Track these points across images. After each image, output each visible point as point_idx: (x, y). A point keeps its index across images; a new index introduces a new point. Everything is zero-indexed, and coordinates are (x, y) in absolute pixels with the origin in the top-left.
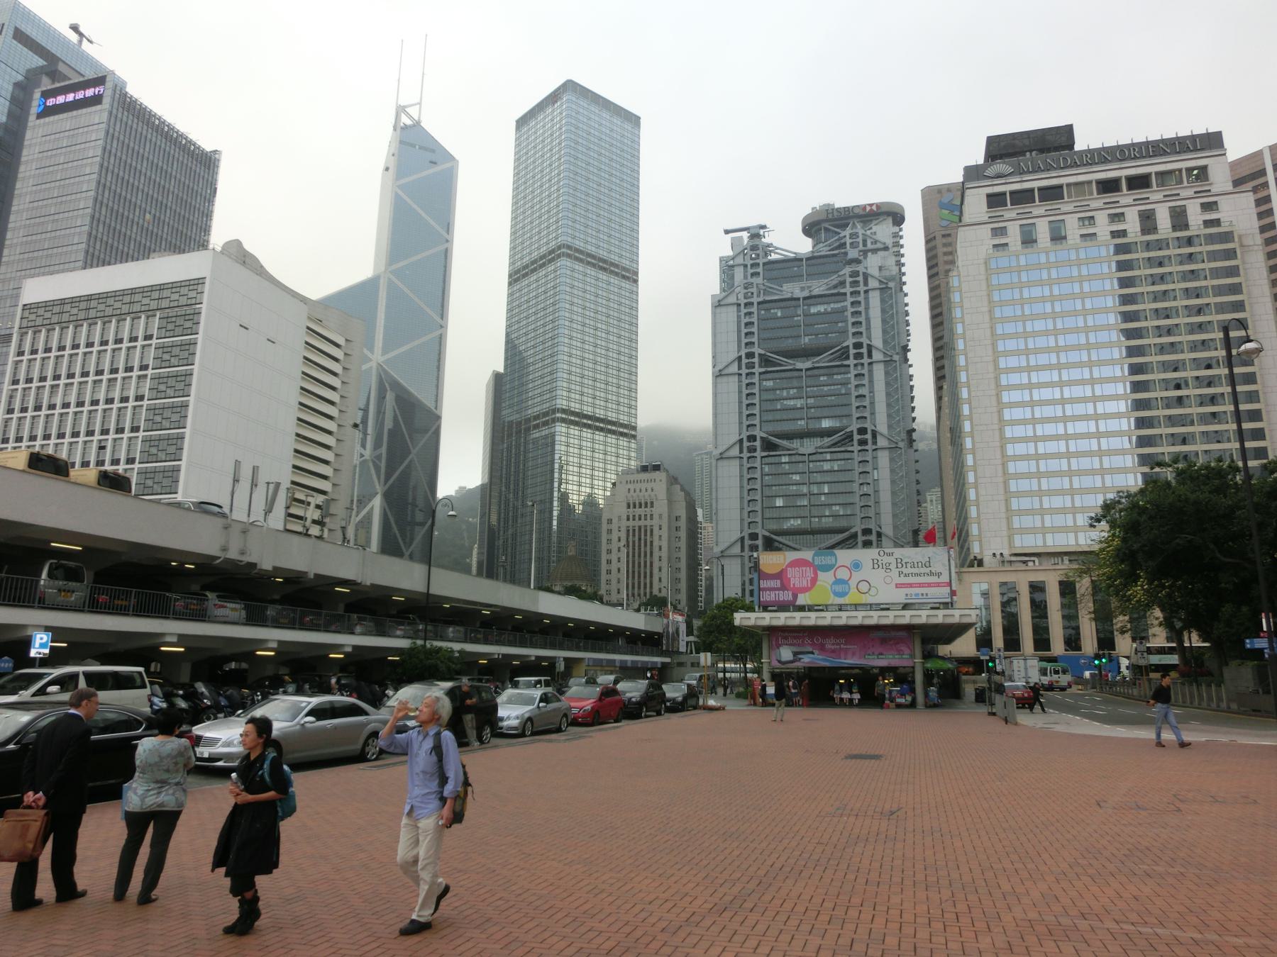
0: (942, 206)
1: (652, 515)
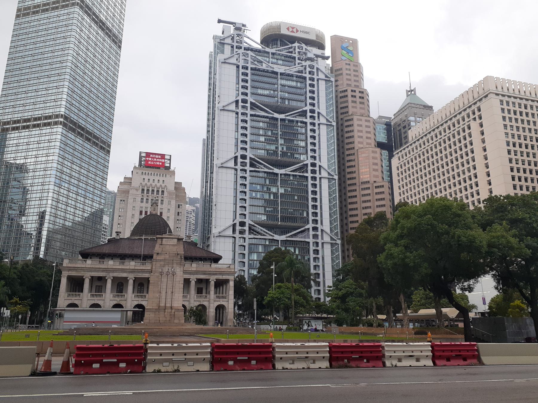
0: (343, 48)
1: (162, 200)
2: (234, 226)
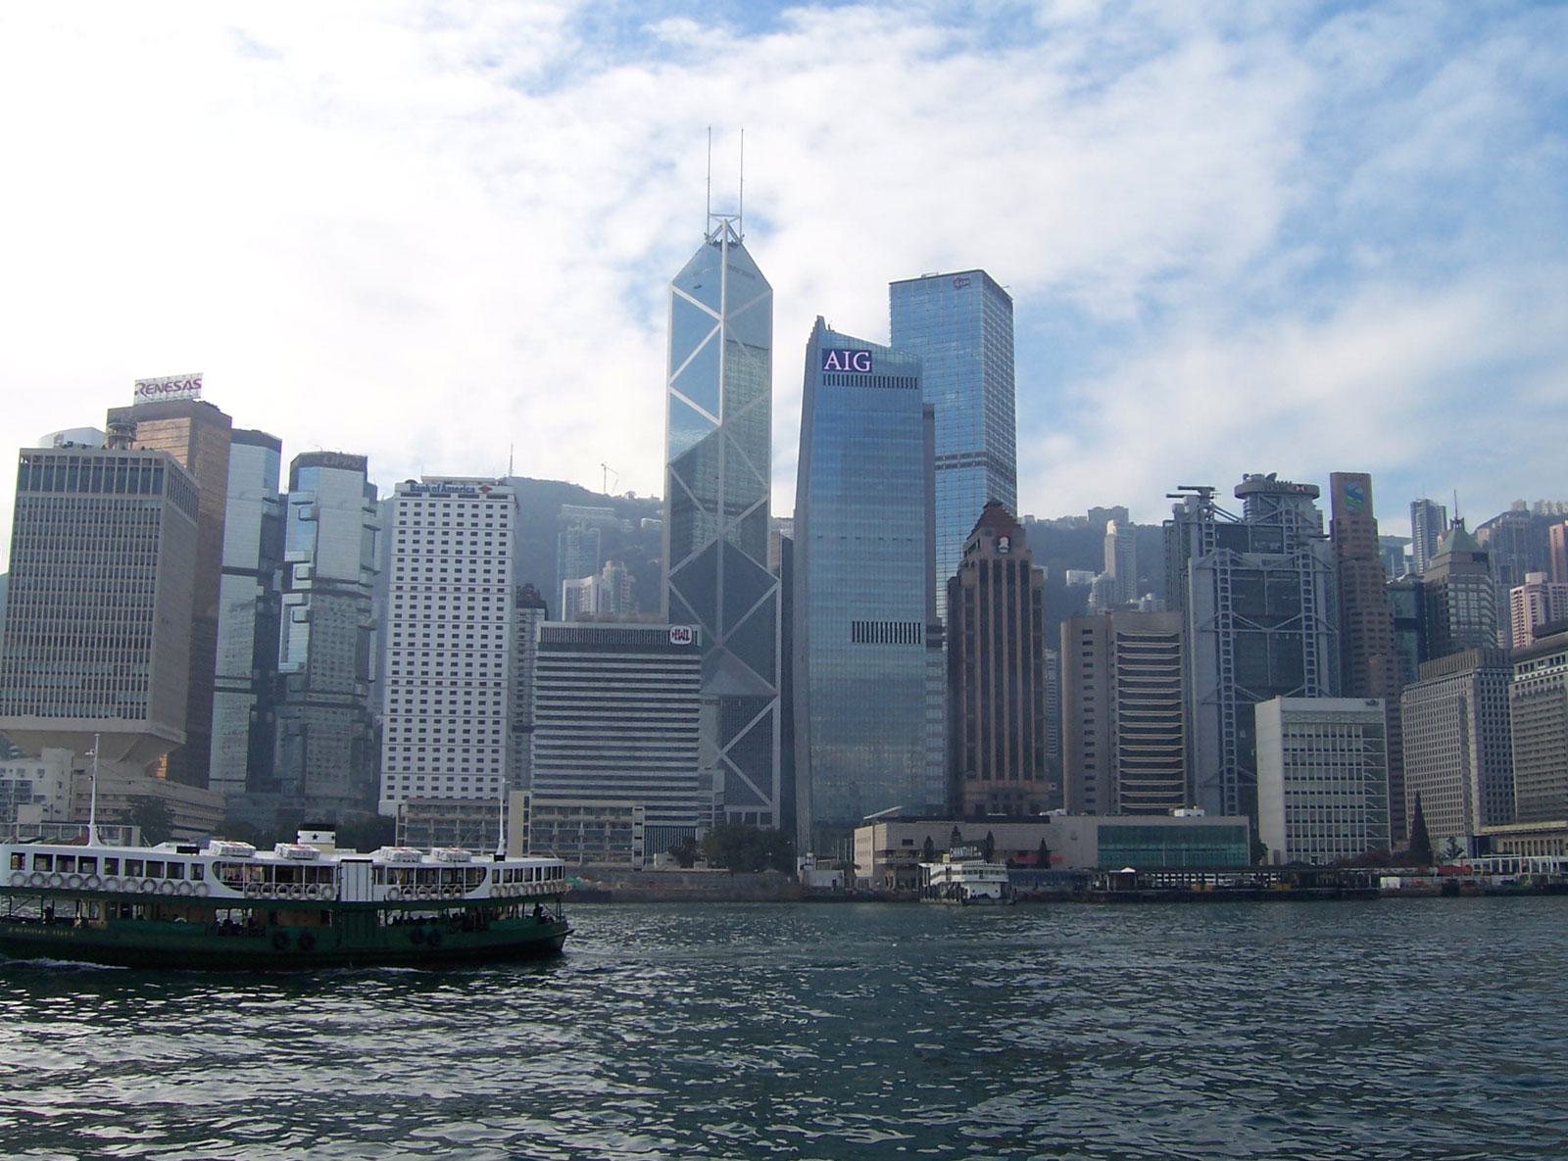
2: (1222, 773)
